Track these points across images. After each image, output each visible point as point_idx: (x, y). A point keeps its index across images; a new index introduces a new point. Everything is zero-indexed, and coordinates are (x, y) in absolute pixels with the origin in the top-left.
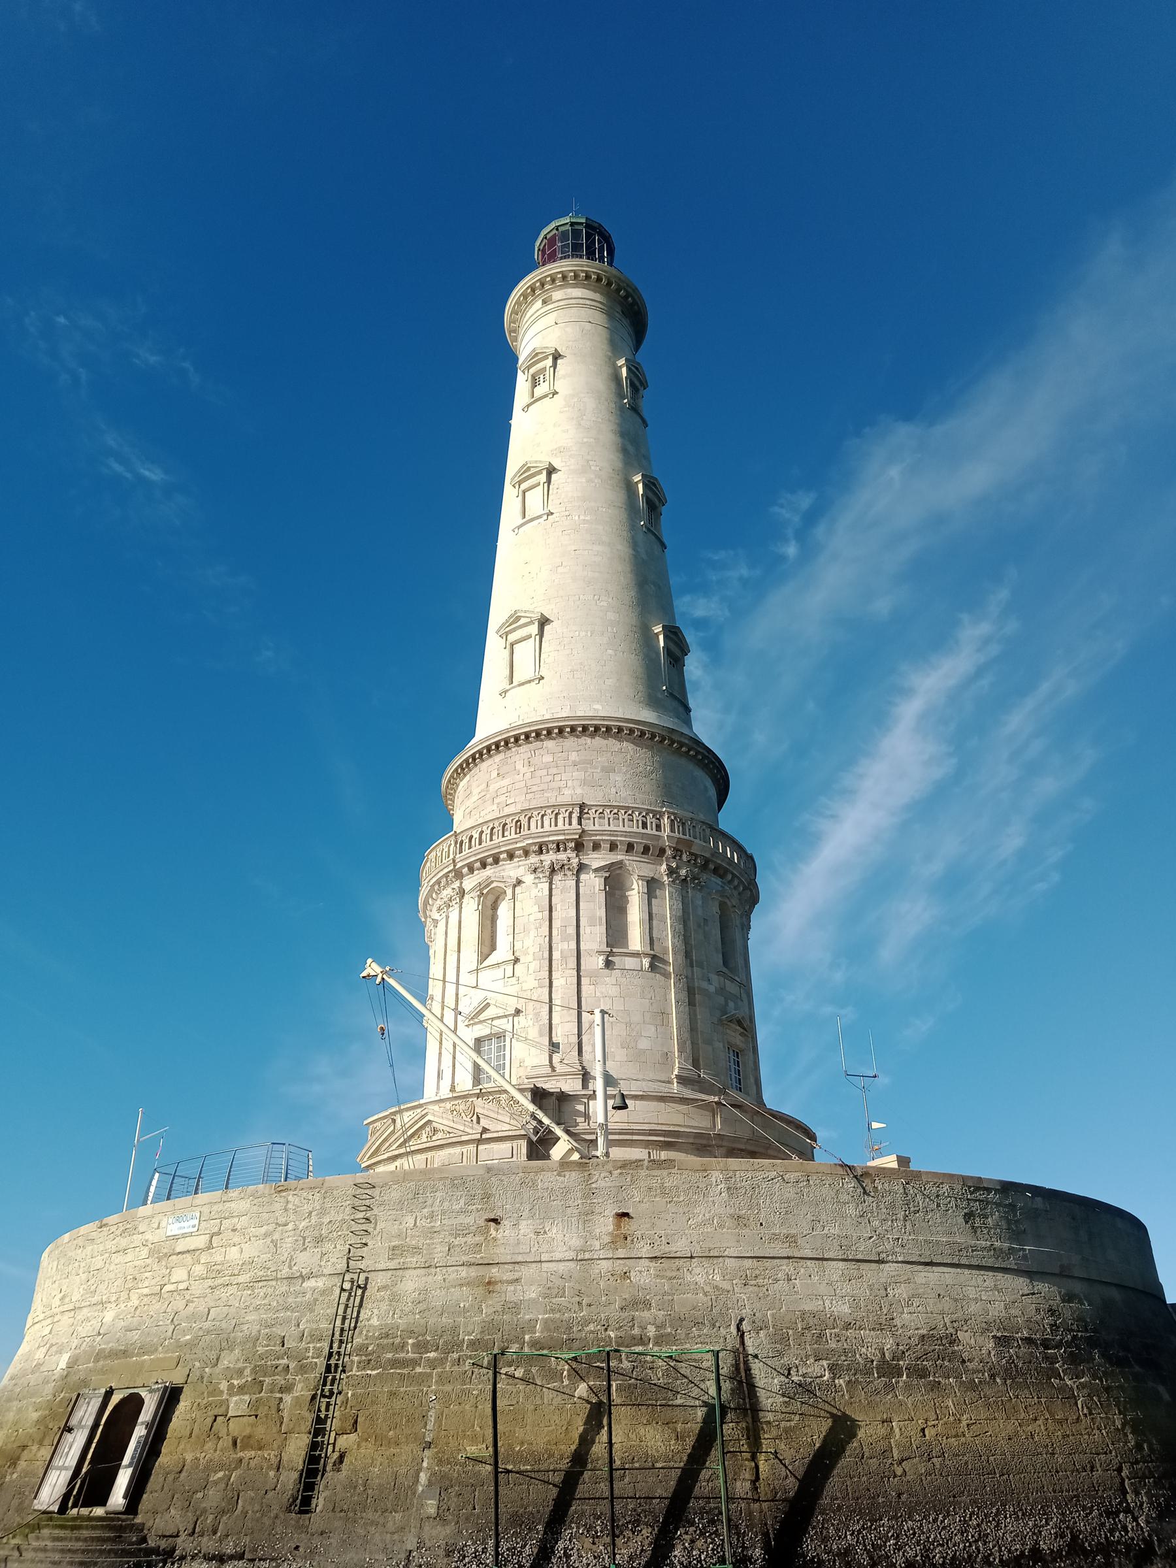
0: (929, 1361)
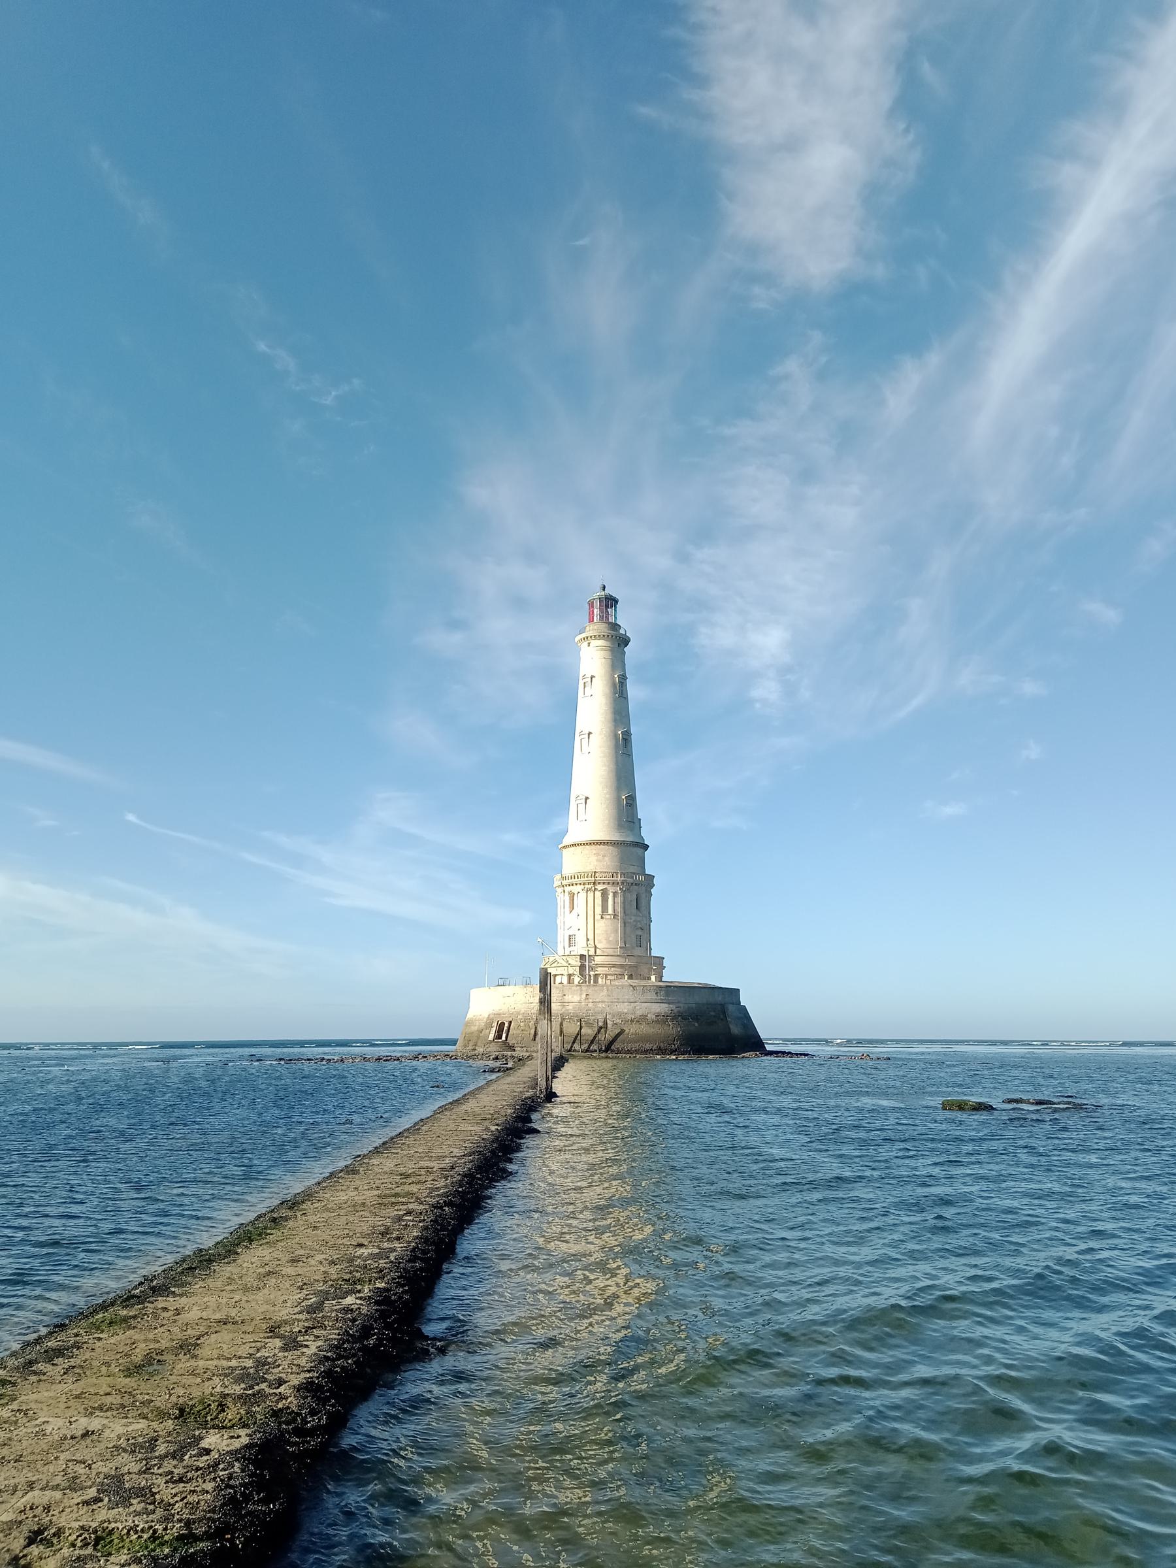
0: (643, 1019)
